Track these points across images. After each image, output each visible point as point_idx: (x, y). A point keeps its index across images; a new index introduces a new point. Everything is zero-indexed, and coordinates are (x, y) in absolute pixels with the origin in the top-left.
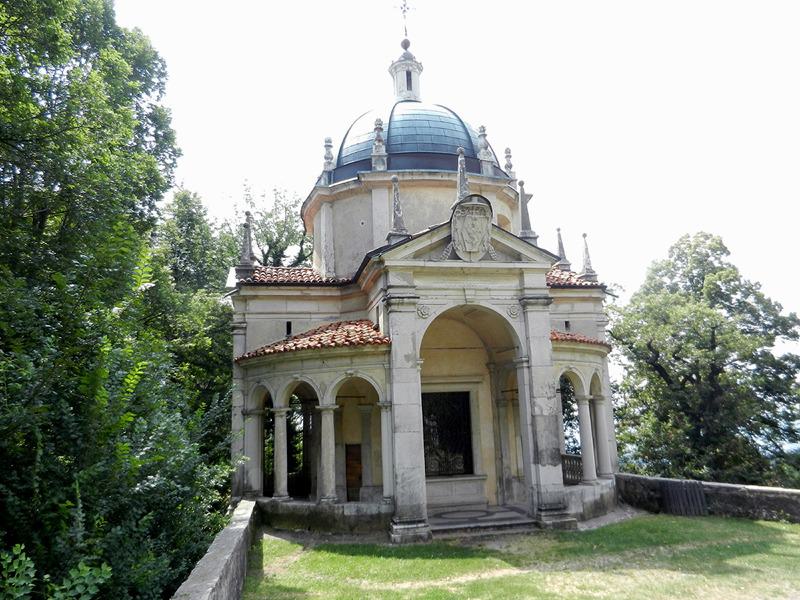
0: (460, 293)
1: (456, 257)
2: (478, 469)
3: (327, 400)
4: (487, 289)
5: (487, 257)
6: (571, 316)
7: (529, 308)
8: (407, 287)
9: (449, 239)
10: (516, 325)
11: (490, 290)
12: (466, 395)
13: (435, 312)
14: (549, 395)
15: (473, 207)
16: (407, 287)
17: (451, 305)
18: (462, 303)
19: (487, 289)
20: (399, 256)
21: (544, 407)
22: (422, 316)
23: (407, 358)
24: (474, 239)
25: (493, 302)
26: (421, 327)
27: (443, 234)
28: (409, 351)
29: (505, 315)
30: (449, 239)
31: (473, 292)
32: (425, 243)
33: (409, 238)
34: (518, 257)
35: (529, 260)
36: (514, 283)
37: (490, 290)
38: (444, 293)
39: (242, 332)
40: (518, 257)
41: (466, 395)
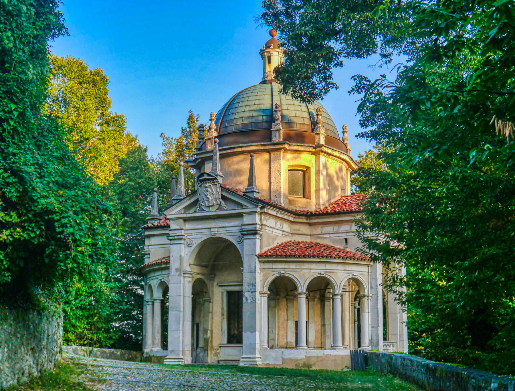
0: (209, 230)
4: (224, 227)
5: (220, 208)
6: (348, 234)
7: (245, 237)
8: (178, 230)
9: (197, 201)
10: (238, 246)
11: (226, 227)
13: (196, 243)
14: (252, 290)
15: (205, 180)
16: (178, 230)
17: (205, 238)
18: (210, 236)
19: (224, 227)
20: (173, 212)
21: (248, 297)
22: (189, 246)
23: (177, 270)
24: (208, 198)
25: (228, 234)
29: (234, 242)
31: (216, 230)
32: (188, 202)
35: (247, 207)
36: (236, 222)
37: (226, 227)
38: (201, 231)
39: (148, 256)
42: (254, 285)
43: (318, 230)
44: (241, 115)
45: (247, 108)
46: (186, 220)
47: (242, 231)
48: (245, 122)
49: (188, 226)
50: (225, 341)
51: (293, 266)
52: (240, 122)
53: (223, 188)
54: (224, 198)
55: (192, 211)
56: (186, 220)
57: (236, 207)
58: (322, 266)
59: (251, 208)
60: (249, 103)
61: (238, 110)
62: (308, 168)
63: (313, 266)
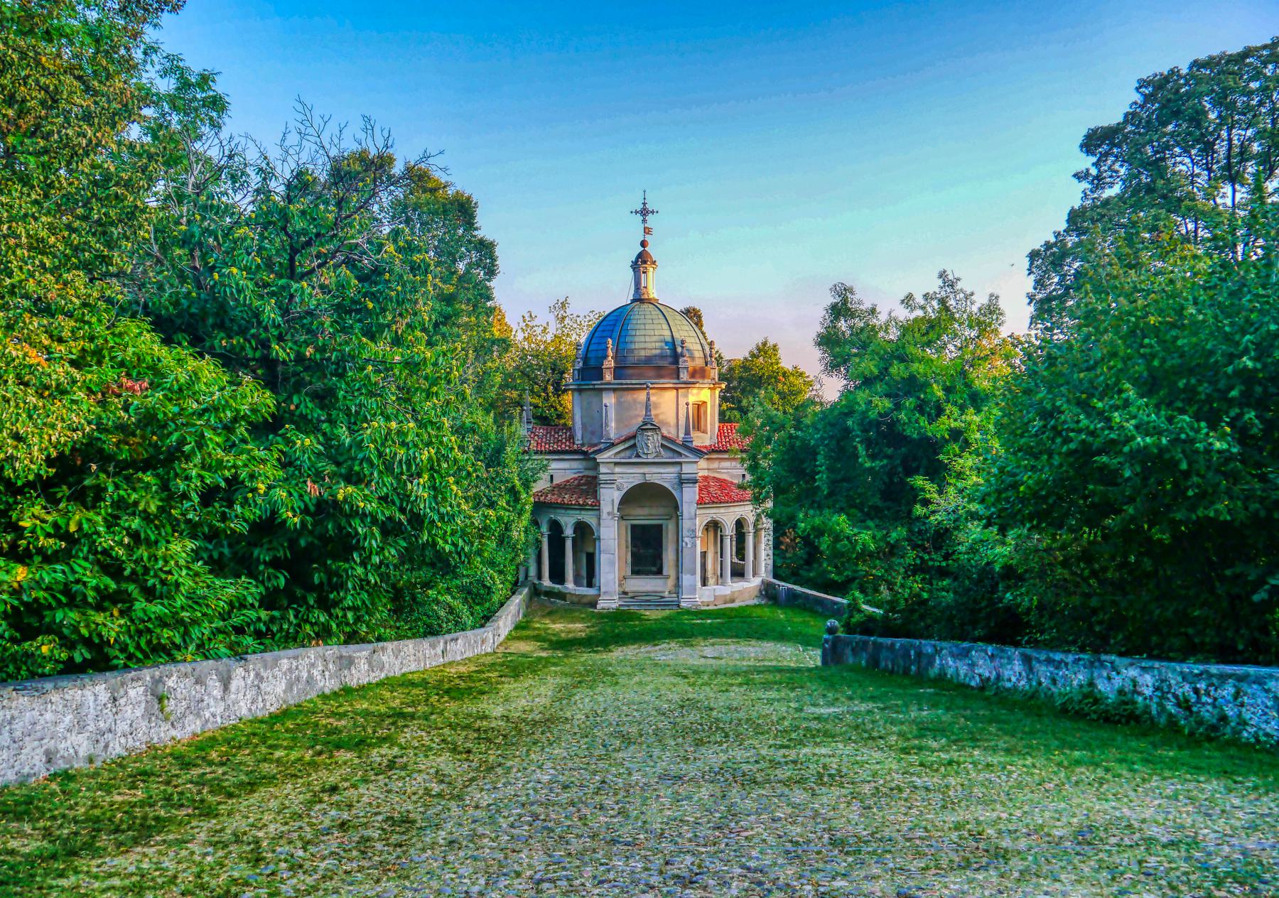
1: (638, 456)
2: (665, 573)
3: (569, 532)
9: (634, 446)
12: (660, 526)
13: (627, 487)
22: (618, 489)
26: (617, 496)
27: (631, 443)
28: (609, 509)
30: (634, 446)
32: (621, 447)
33: (613, 445)
34: (680, 454)
40: (680, 454)
41: (660, 526)
42: (694, 531)
43: (715, 465)
44: (642, 345)
45: (648, 339)
46: (616, 464)
47: (680, 479)
48: (649, 353)
49: (617, 469)
50: (629, 573)
51: (722, 510)
52: (643, 353)
53: (664, 437)
54: (663, 446)
55: (622, 455)
56: (616, 464)
57: (670, 454)
58: (741, 509)
59: (692, 458)
60: (648, 332)
61: (636, 339)
62: (705, 403)
63: (736, 509)
